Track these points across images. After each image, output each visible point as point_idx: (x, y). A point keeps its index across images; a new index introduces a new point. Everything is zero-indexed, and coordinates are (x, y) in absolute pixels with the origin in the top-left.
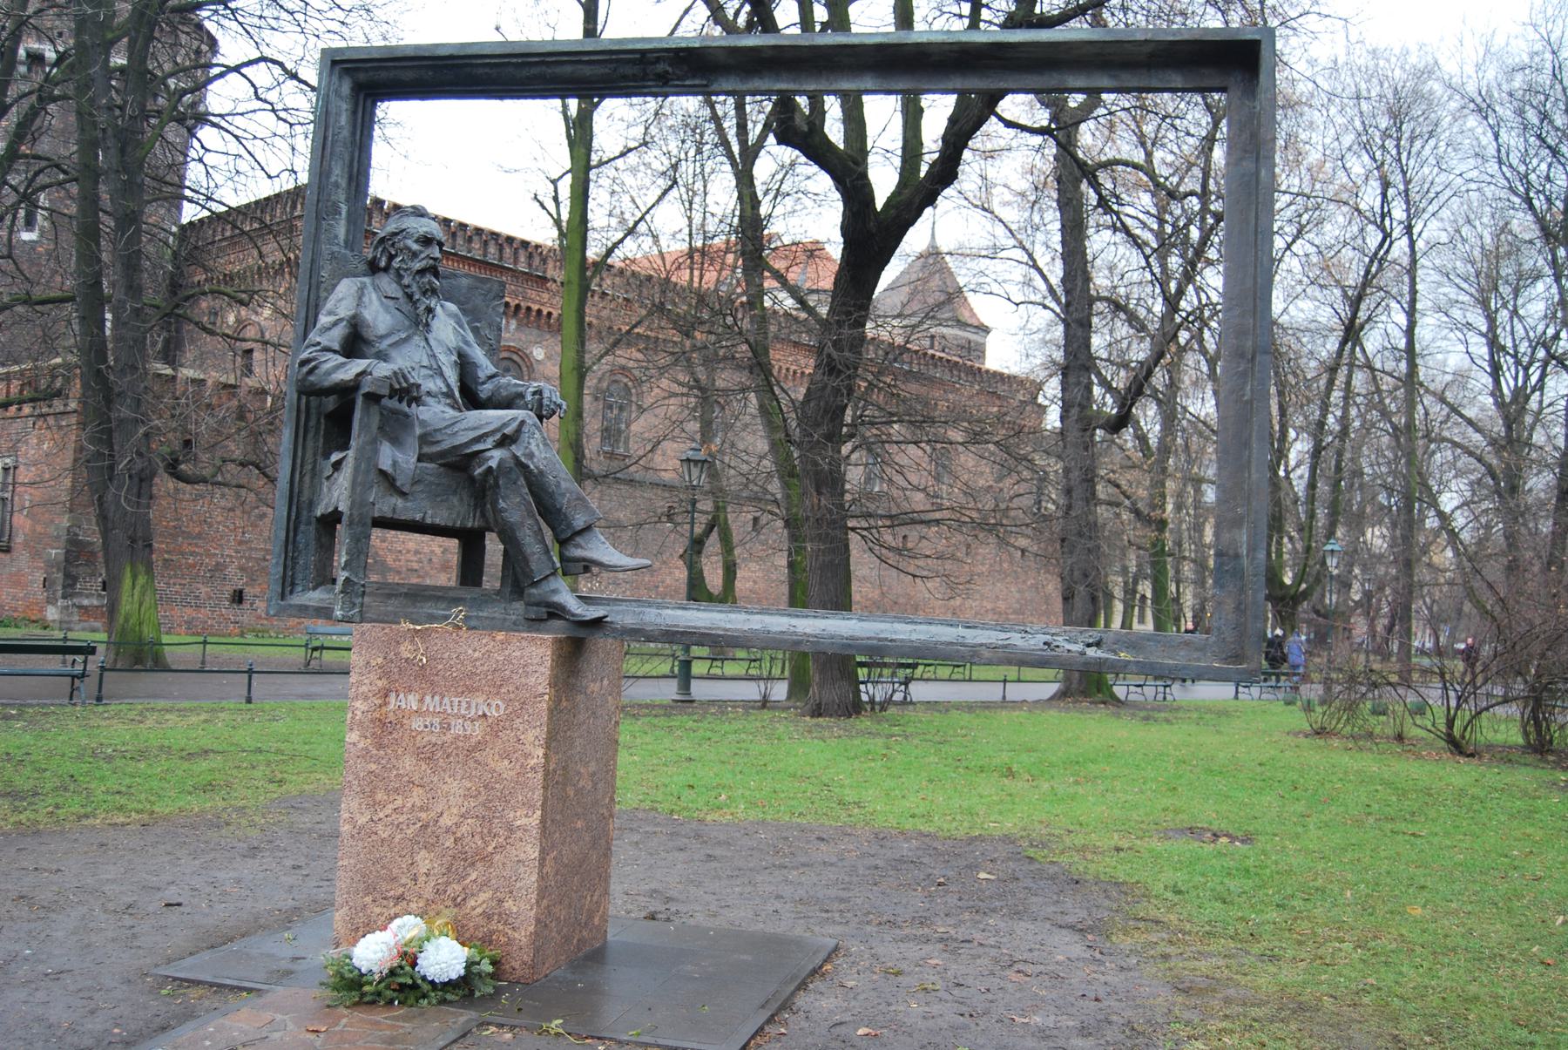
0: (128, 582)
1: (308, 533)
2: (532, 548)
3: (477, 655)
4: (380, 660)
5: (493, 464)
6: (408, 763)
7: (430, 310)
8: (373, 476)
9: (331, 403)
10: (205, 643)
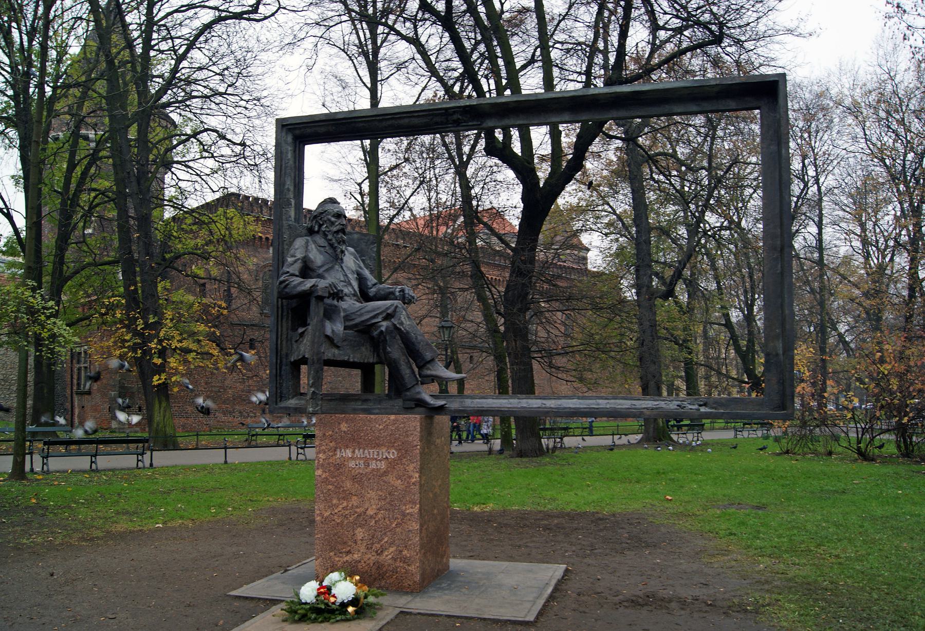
0: (157, 406)
1: (286, 369)
2: (405, 371)
5: (383, 329)
6: (348, 484)
7: (342, 252)
9: (294, 303)
10: (197, 435)
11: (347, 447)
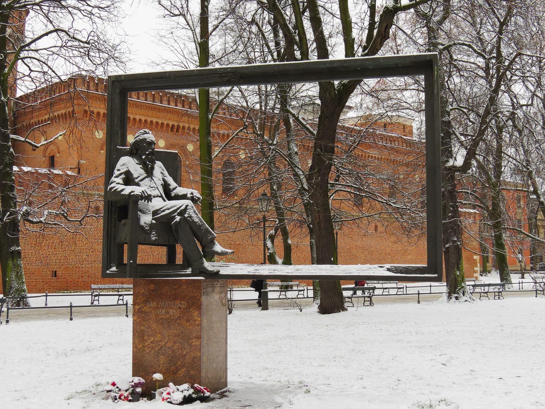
10: (46, 296)
11: (153, 301)
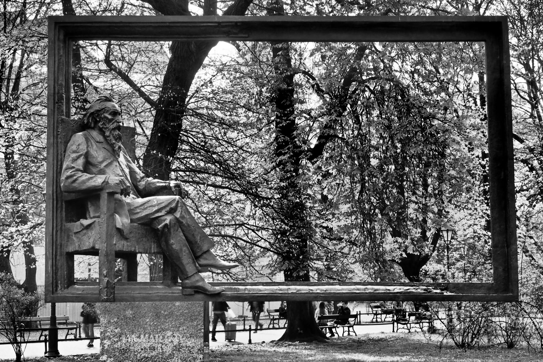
3: (166, 313)
4: (115, 320)
5: (167, 222)
8: (114, 231)
